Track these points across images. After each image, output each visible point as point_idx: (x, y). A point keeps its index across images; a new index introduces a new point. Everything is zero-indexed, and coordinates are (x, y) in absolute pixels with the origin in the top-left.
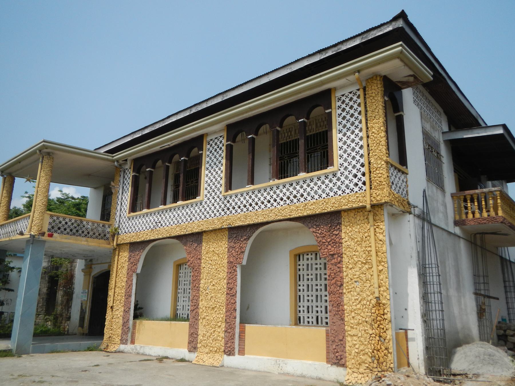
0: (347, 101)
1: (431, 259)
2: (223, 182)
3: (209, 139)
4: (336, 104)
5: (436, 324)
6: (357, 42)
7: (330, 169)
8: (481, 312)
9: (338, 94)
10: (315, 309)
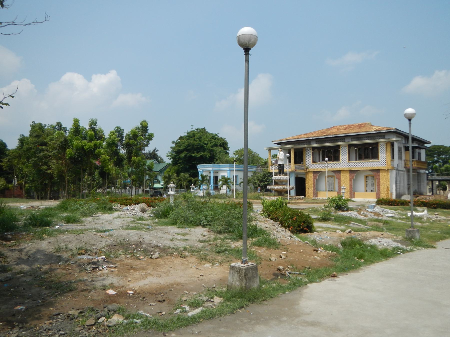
0: (382, 146)
1: (398, 178)
2: (347, 158)
3: (341, 146)
4: (379, 146)
5: (398, 191)
6: (385, 131)
7: (378, 160)
8: (409, 189)
9: (380, 144)
10: (371, 189)
